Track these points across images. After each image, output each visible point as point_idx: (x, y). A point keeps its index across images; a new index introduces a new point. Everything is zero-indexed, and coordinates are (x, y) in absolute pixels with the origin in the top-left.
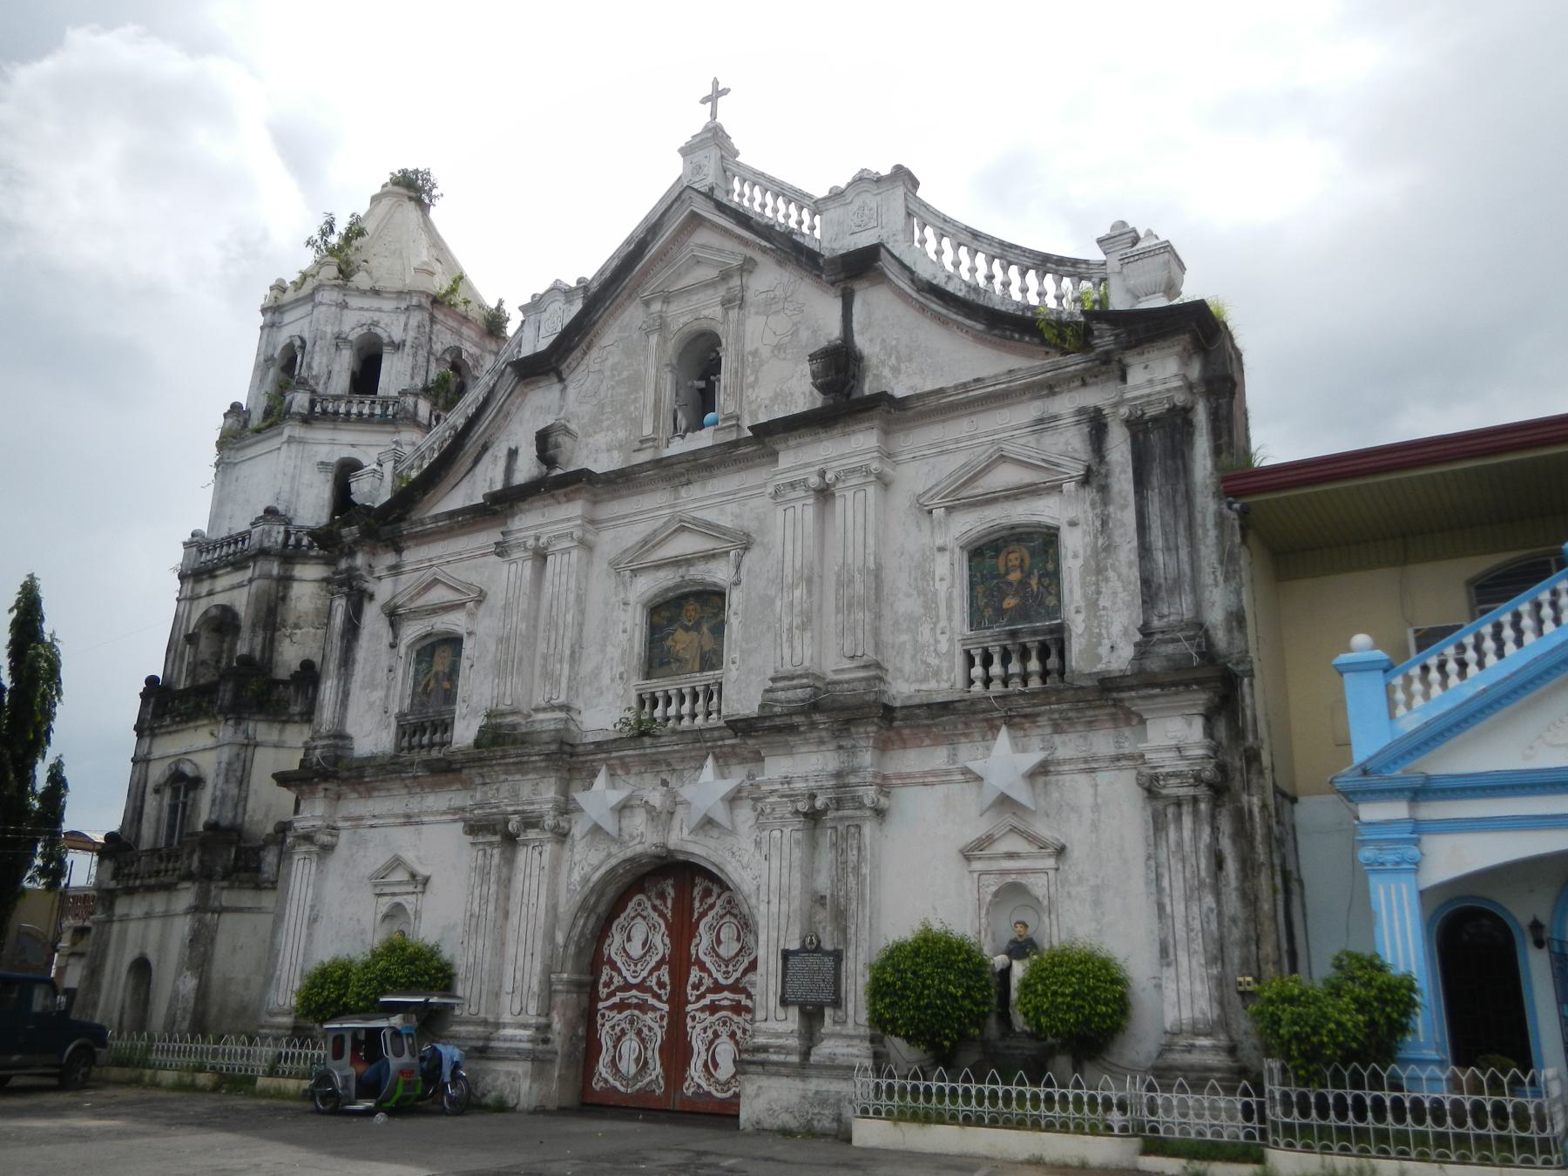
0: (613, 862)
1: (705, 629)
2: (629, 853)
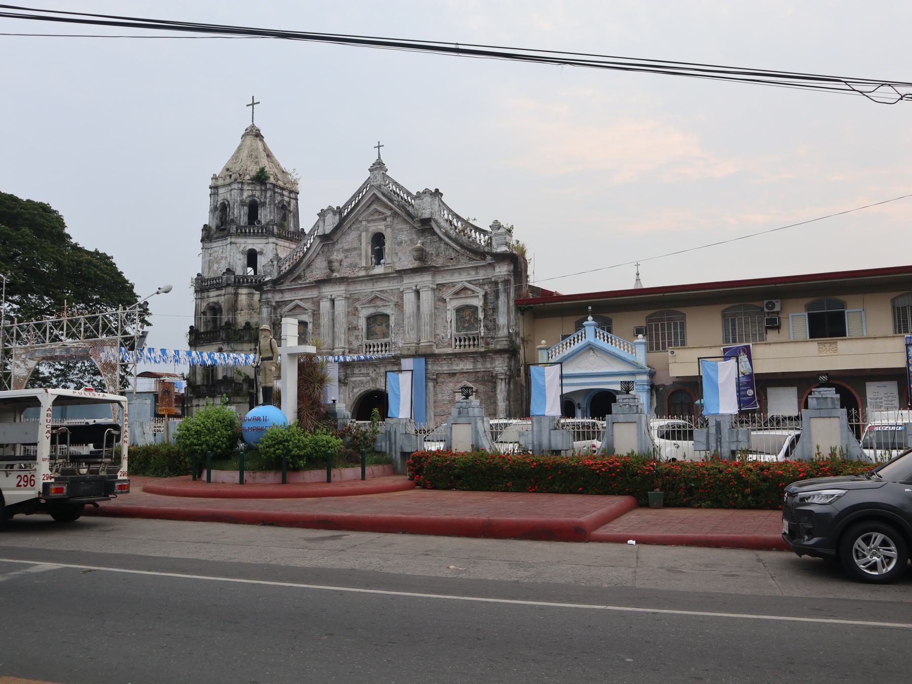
0: (362, 391)
1: (384, 325)
2: (366, 389)
